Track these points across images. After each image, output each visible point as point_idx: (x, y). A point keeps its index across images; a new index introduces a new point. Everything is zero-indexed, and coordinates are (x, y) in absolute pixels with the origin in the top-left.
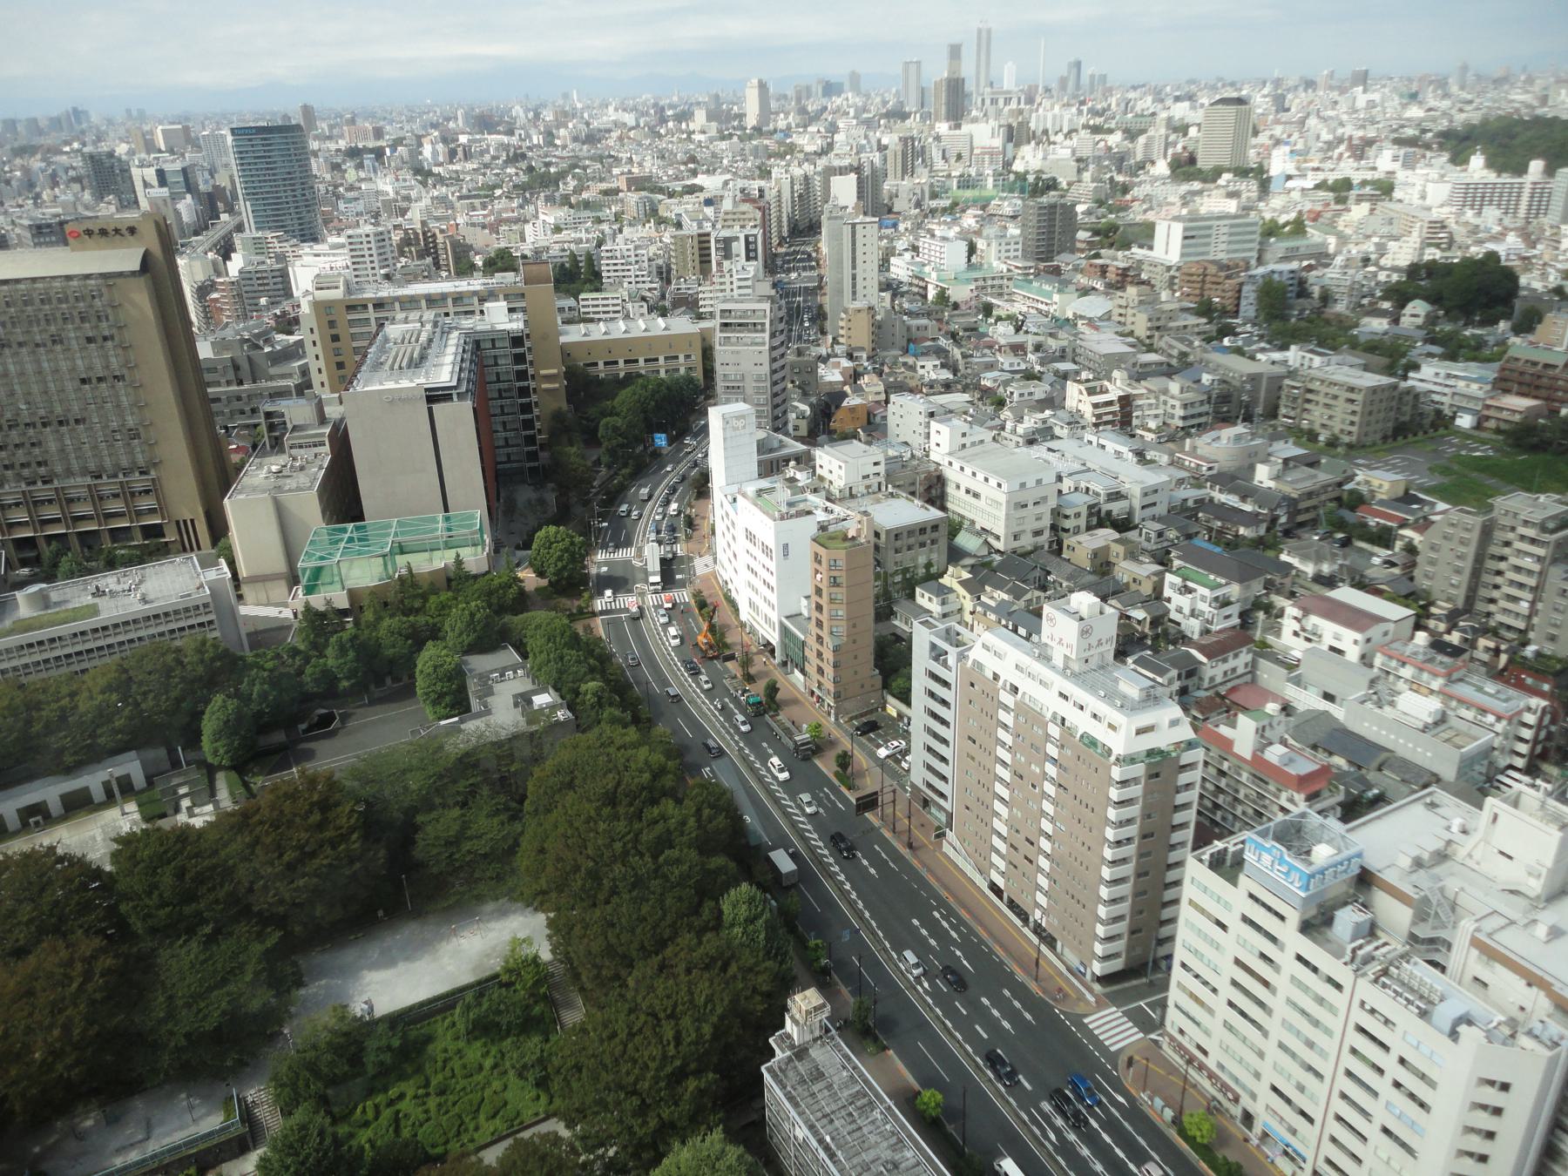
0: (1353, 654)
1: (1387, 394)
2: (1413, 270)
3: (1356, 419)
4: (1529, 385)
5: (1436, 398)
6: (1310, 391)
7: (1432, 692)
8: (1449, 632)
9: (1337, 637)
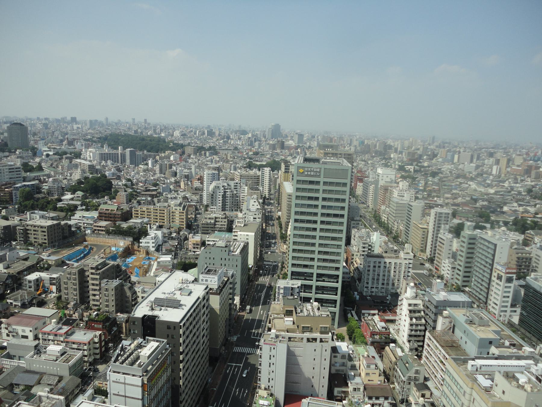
0: (31, 336)
1: (56, 227)
2: (79, 182)
3: (46, 237)
4: (108, 217)
5: (80, 224)
6: (28, 230)
7: (62, 342)
8: (74, 314)
9: (24, 331)
